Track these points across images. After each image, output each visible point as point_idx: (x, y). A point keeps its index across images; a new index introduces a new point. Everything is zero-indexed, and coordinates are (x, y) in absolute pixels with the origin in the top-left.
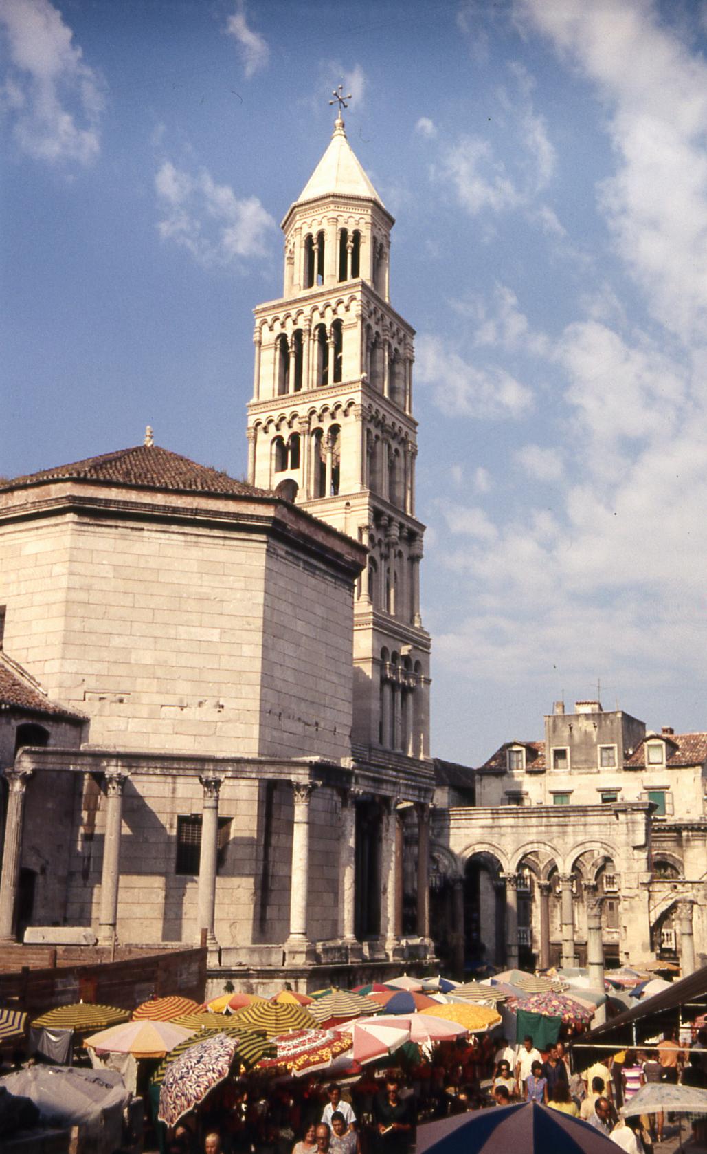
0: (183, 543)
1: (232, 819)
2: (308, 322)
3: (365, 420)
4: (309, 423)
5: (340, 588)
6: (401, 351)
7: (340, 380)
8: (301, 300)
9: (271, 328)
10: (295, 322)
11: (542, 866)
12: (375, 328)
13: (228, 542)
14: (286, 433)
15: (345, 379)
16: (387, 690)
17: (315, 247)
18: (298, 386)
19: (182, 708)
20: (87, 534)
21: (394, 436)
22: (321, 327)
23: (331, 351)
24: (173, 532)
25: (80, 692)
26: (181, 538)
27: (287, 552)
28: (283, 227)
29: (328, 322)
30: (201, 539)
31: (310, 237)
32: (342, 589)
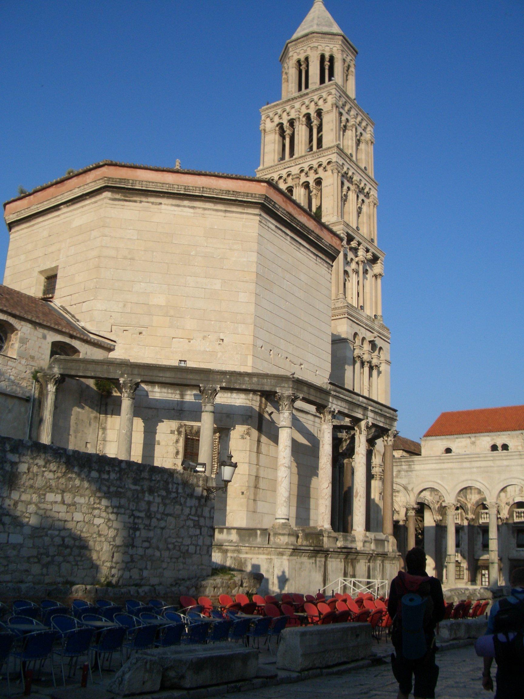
0: (193, 215)
2: (298, 113)
4: (299, 178)
5: (320, 265)
7: (321, 147)
8: (293, 99)
10: (288, 114)
11: (469, 506)
13: (228, 214)
15: (324, 146)
17: (303, 67)
19: (189, 340)
20: (117, 206)
22: (308, 116)
24: (185, 206)
26: (191, 210)
27: (276, 227)
28: (280, 61)
29: (312, 111)
30: (206, 212)
31: (299, 62)
32: (321, 266)
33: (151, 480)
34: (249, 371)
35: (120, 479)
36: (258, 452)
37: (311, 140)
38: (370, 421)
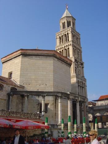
1: (49, 104)
3: (72, 46)
6: (78, 37)
9: (58, 36)
10: (62, 34)
12: (74, 34)
14: (61, 50)
15: (69, 41)
16: (79, 87)
18: (63, 43)
21: (78, 49)
22: (65, 34)
23: (67, 37)
25: (23, 83)
29: (66, 33)
33: (27, 116)
34: (52, 91)
35: (20, 116)
36: (55, 108)
37: (66, 40)
38: (79, 100)
